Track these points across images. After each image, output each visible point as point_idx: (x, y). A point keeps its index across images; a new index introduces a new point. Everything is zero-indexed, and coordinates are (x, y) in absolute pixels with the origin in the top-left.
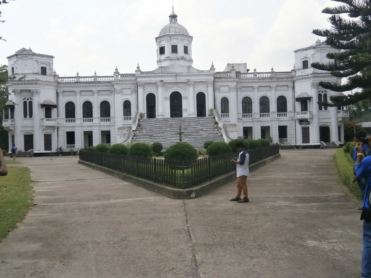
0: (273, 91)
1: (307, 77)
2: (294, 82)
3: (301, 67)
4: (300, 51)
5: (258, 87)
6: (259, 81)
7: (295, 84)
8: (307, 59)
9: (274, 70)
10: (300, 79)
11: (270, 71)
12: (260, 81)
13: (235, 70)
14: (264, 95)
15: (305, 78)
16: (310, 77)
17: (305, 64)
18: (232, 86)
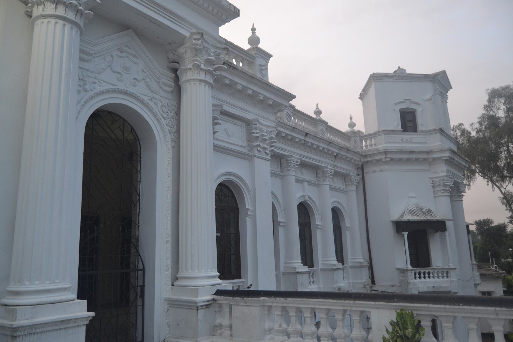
0: (326, 188)
1: (425, 156)
2: (362, 168)
3: (398, 125)
4: (391, 80)
5: (299, 162)
6: (302, 138)
7: (367, 176)
8: (413, 106)
9: (323, 117)
10: (400, 159)
11: (314, 116)
12: (307, 139)
13: (271, 56)
14: (307, 198)
15: (417, 160)
16: (434, 159)
17: (408, 121)
18: (265, 129)
